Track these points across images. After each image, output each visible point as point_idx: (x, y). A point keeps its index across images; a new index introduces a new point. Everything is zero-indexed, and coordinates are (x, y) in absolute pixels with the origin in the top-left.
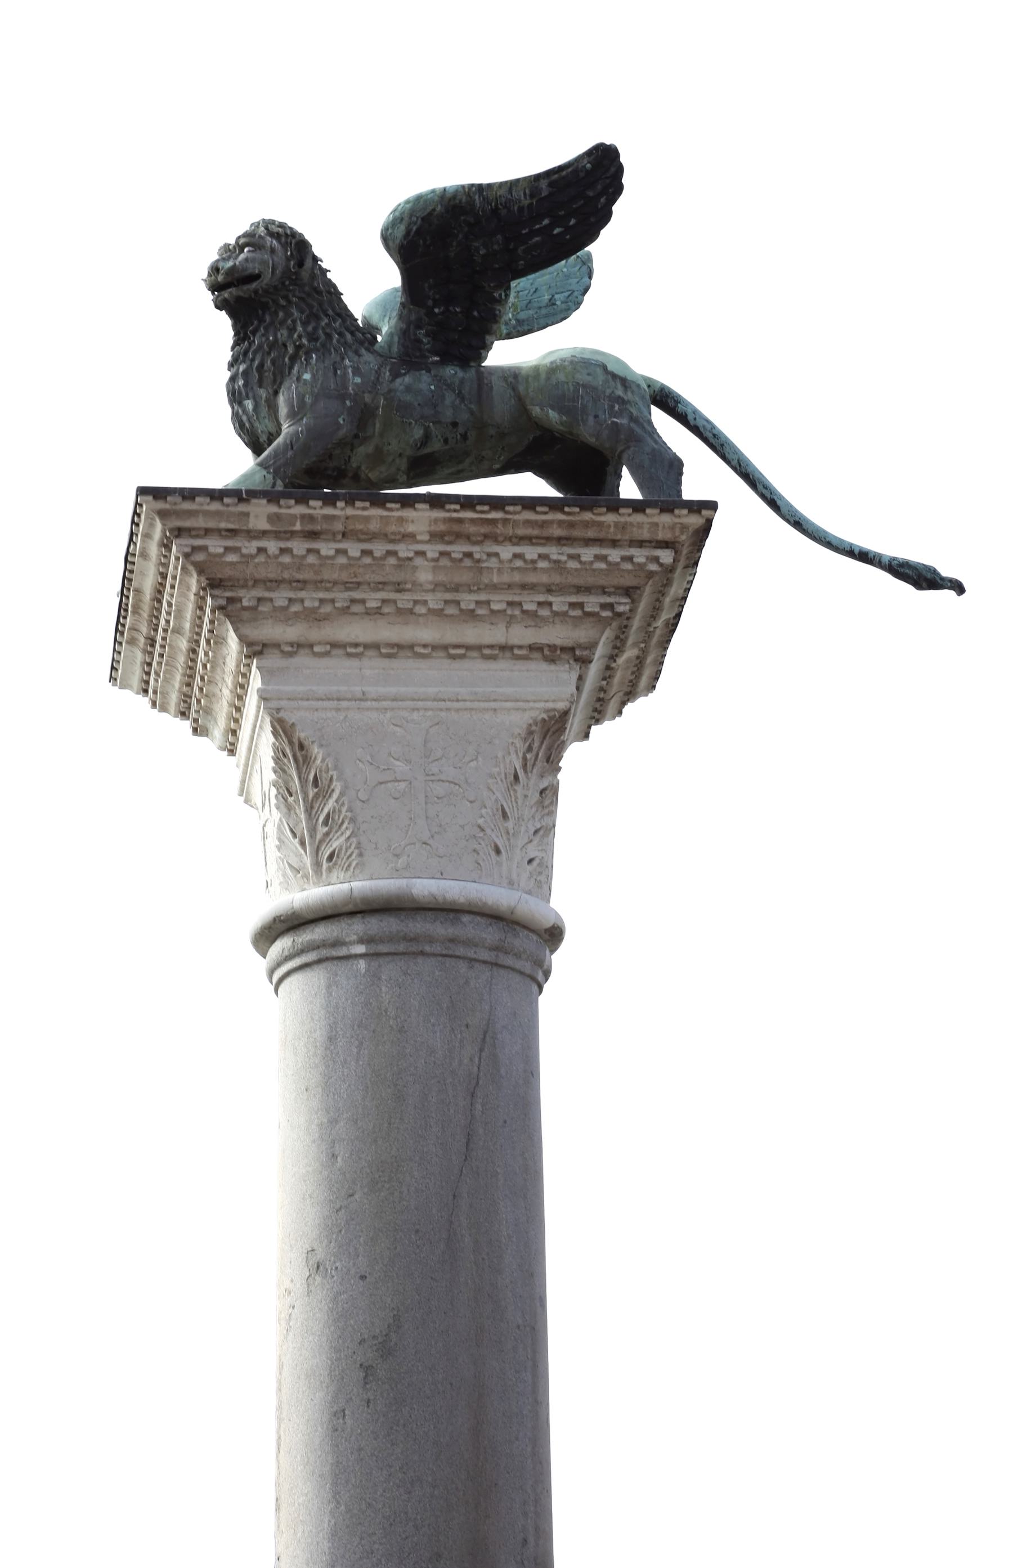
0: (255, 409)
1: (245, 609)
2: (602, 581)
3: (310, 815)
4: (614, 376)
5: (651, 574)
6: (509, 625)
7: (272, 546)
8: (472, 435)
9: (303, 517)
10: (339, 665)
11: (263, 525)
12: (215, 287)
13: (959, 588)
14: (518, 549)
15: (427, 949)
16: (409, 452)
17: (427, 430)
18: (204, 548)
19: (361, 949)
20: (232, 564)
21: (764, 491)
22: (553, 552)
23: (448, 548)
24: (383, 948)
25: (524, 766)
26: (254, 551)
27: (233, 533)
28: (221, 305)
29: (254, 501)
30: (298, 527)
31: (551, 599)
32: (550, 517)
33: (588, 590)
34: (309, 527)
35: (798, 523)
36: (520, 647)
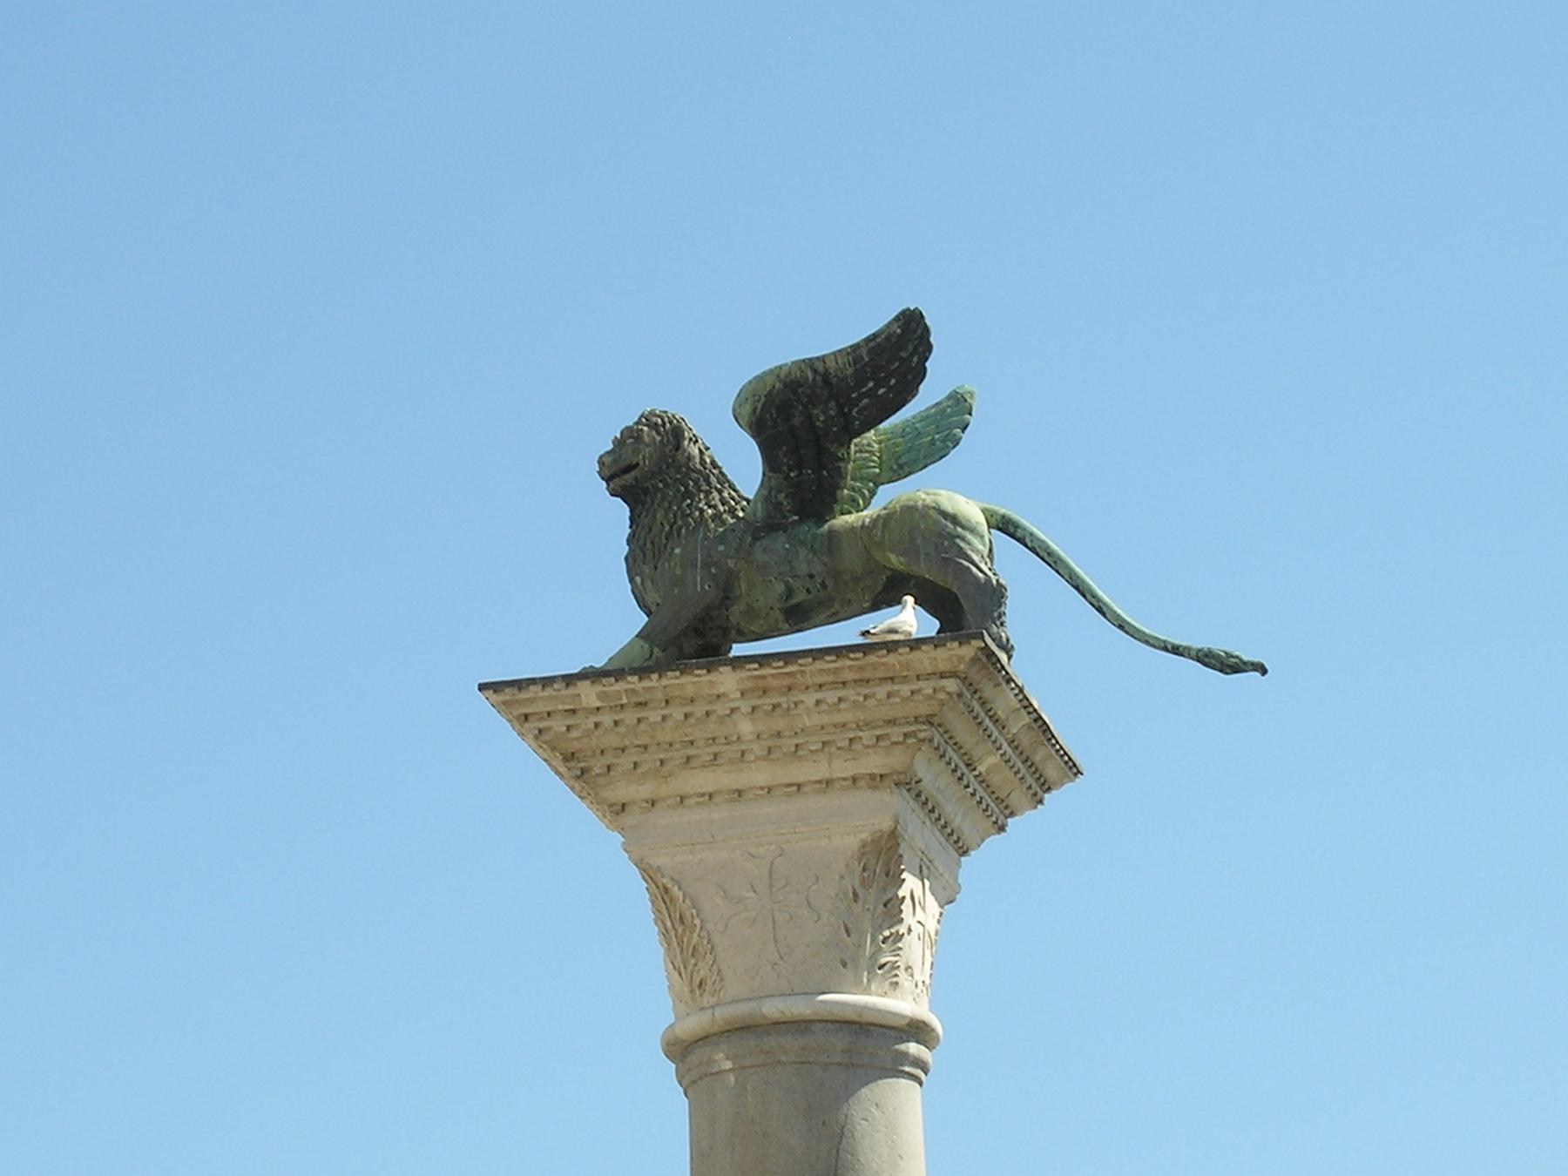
1: (598, 775)
2: (897, 712)
4: (945, 515)
5: (942, 704)
7: (607, 719)
8: (829, 582)
10: (693, 816)
12: (608, 480)
13: (1264, 671)
14: (819, 695)
15: (783, 1059)
16: (777, 605)
18: (549, 728)
19: (728, 1065)
20: (577, 739)
22: (849, 693)
23: (759, 702)
24: (747, 1063)
25: (863, 884)
26: (592, 726)
27: (574, 711)
29: (579, 684)
30: (625, 701)
32: (839, 664)
33: (892, 722)
34: (634, 700)
35: (1122, 626)
36: (844, 779)
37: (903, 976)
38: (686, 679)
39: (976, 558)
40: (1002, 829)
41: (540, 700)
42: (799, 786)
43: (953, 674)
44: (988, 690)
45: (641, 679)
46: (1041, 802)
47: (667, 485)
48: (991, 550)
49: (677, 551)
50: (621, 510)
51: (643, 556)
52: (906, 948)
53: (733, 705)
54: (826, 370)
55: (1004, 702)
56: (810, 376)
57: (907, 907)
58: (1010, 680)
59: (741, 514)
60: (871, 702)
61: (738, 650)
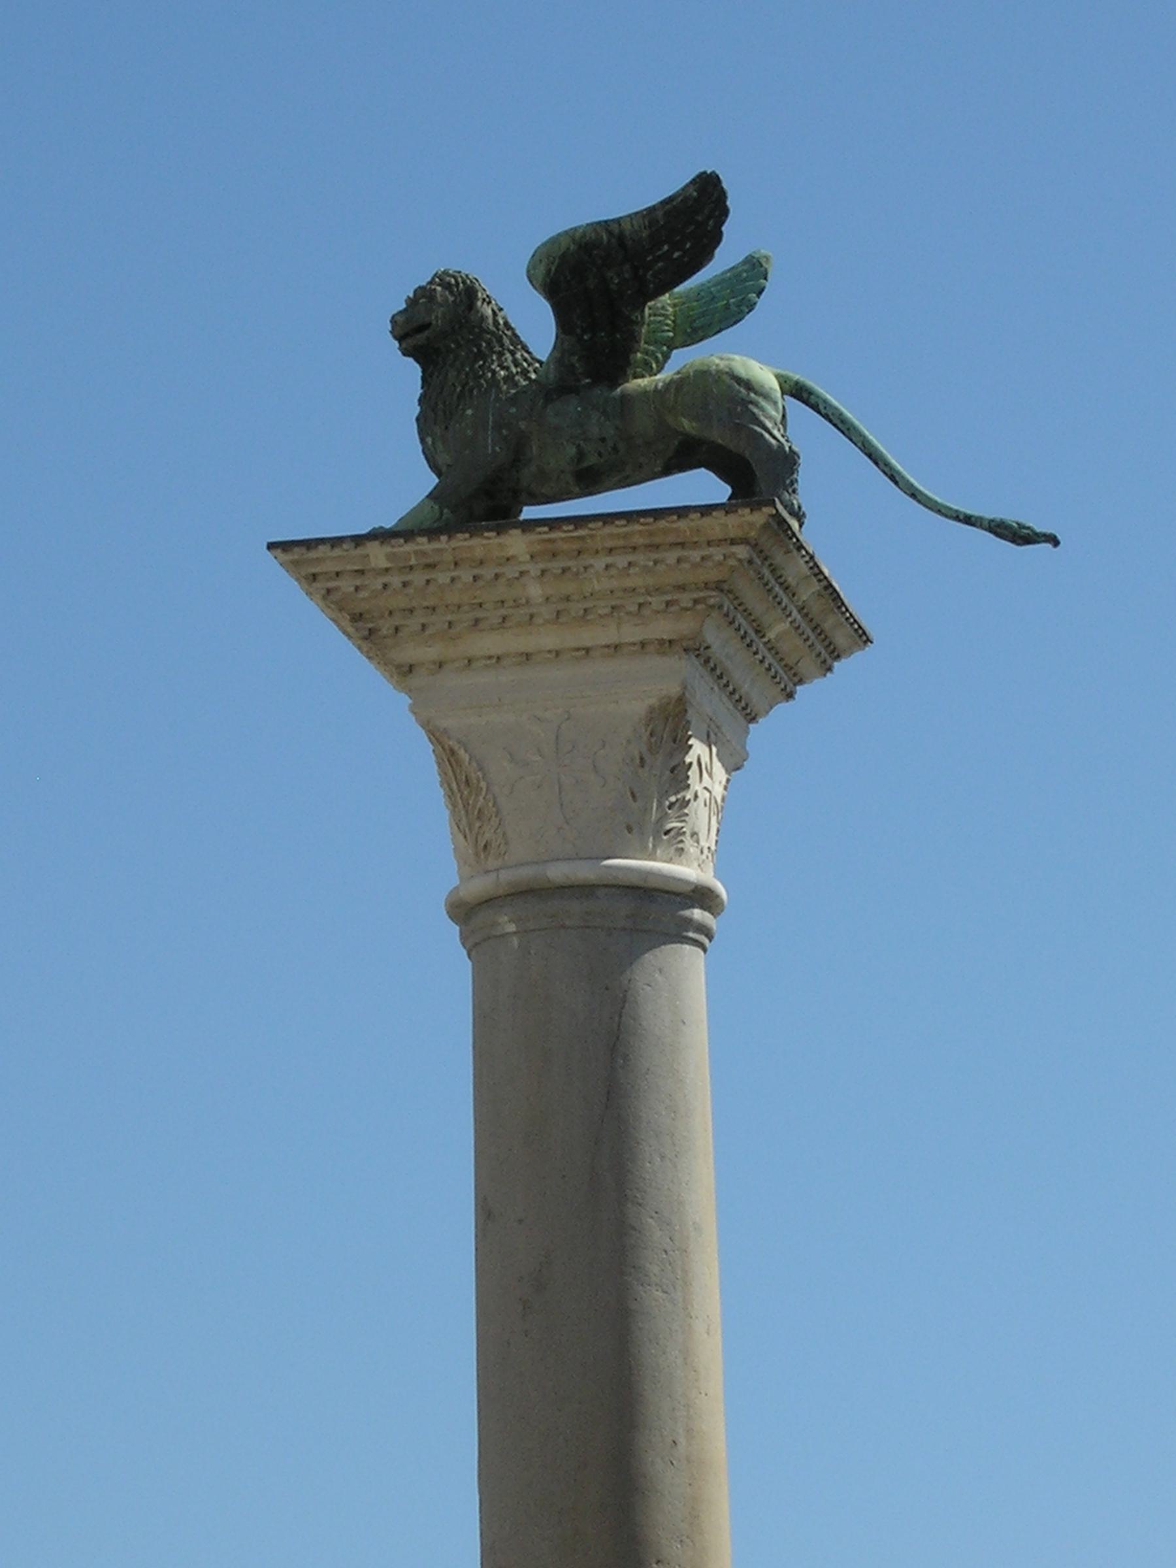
0: (433, 443)
3: (467, 812)
5: (733, 569)
6: (619, 625)
7: (396, 580)
9: (416, 552)
11: (383, 563)
12: (400, 338)
13: (1055, 541)
14: (609, 560)
15: (567, 923)
17: (578, 446)
18: (337, 589)
19: (512, 928)
20: (363, 599)
21: (886, 469)
22: (641, 558)
25: (650, 750)
26: (380, 587)
27: (361, 572)
28: (406, 353)
30: (413, 562)
31: (650, 599)
33: (682, 588)
35: (914, 494)
36: (634, 644)
37: (688, 841)
38: (476, 541)
39: (769, 425)
40: (790, 696)
41: (329, 561)
42: (588, 650)
43: (744, 541)
44: (779, 558)
45: (429, 541)
46: (830, 669)
47: (459, 346)
48: (784, 416)
49: (469, 412)
50: (412, 371)
51: (435, 416)
52: (692, 814)
53: (523, 568)
54: (622, 233)
55: (795, 569)
56: (605, 237)
57: (693, 773)
58: (800, 547)
59: (533, 376)
60: (661, 568)
61: (529, 512)
